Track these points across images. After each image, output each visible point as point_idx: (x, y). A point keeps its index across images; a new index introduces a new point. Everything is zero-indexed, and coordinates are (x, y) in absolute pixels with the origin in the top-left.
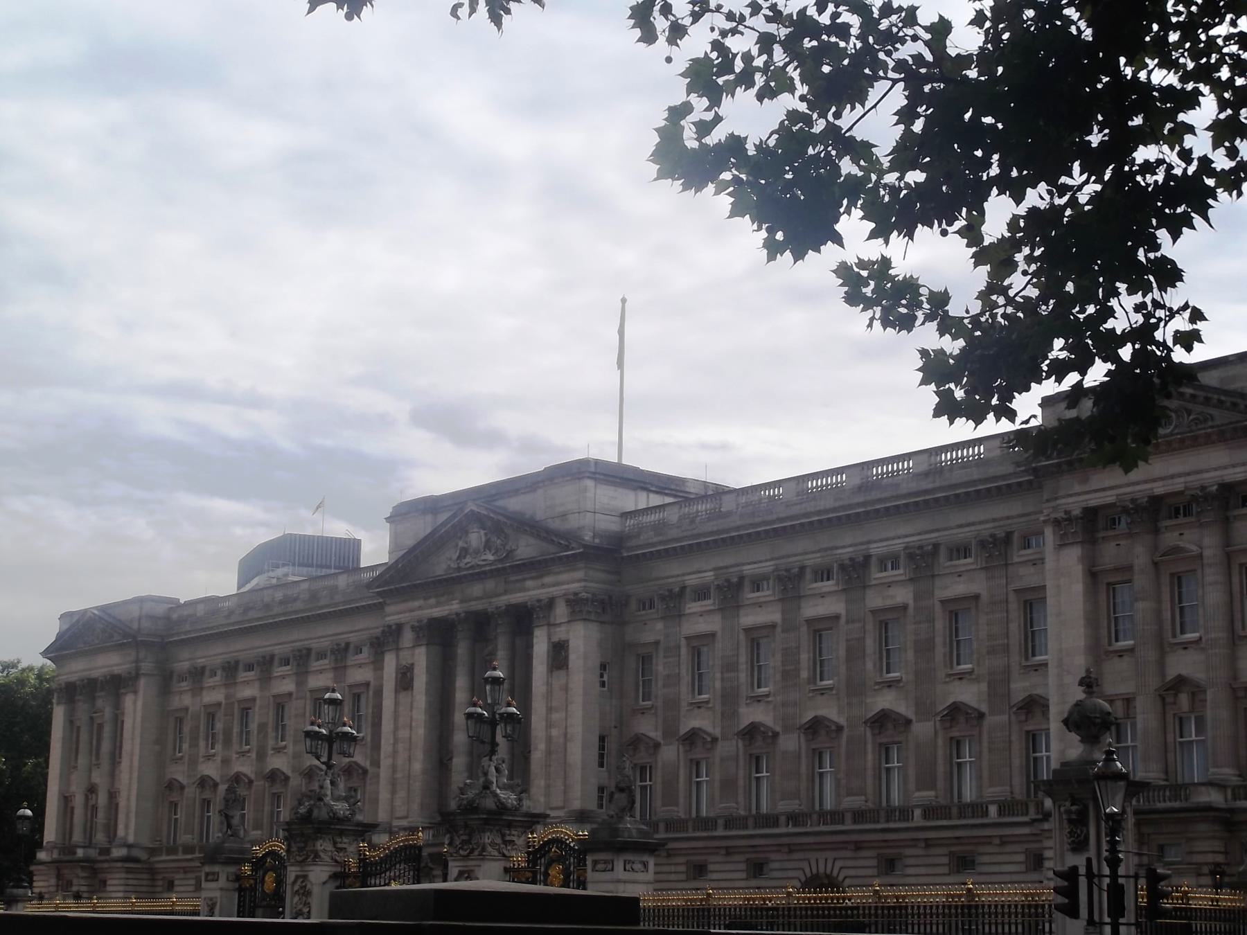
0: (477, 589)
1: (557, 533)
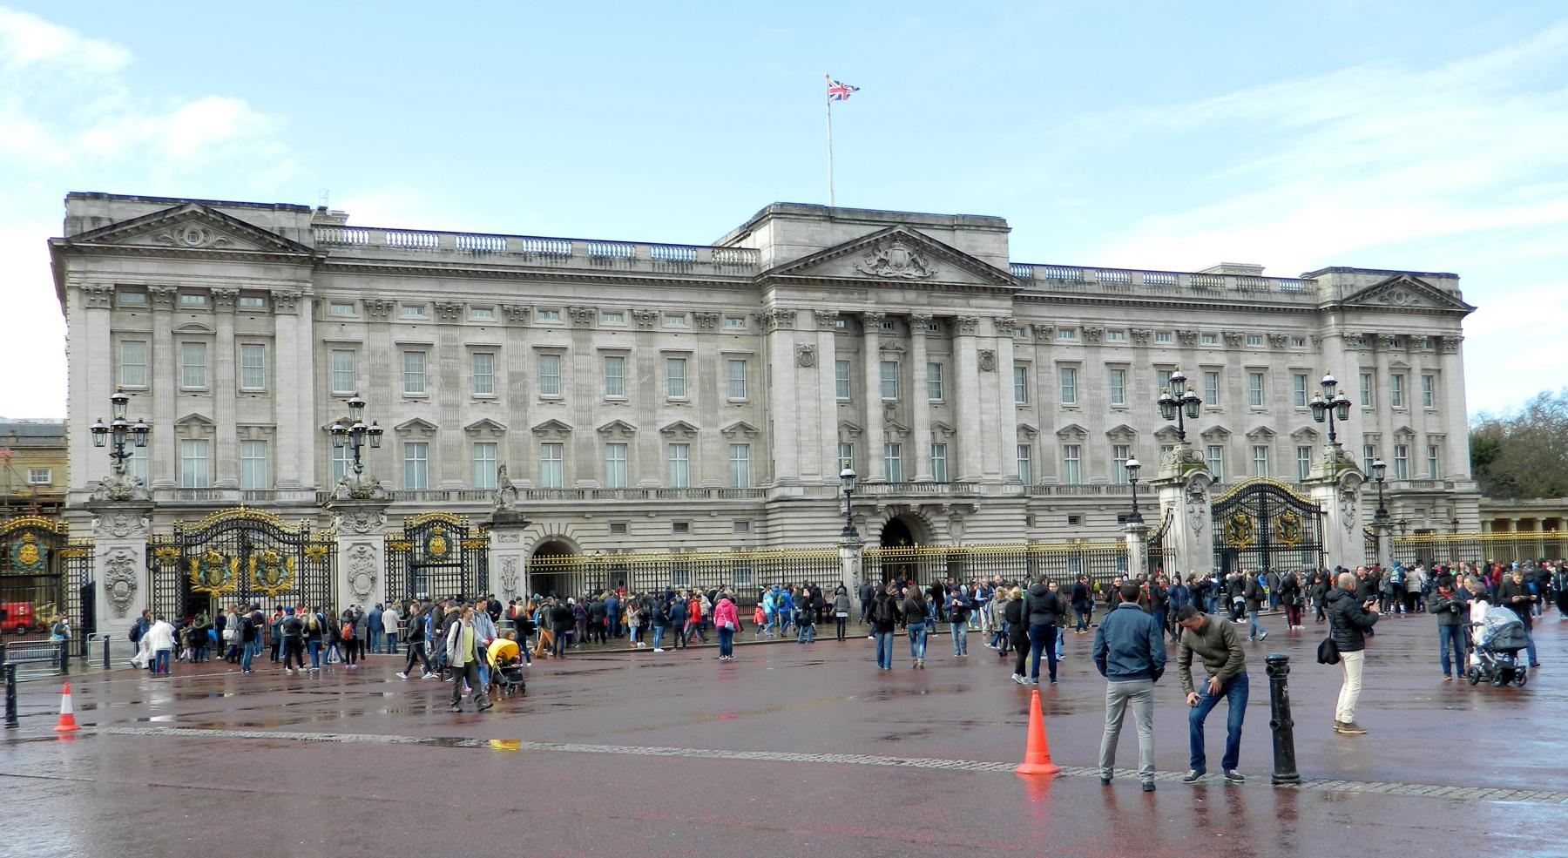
0: (896, 296)
1: (1000, 271)
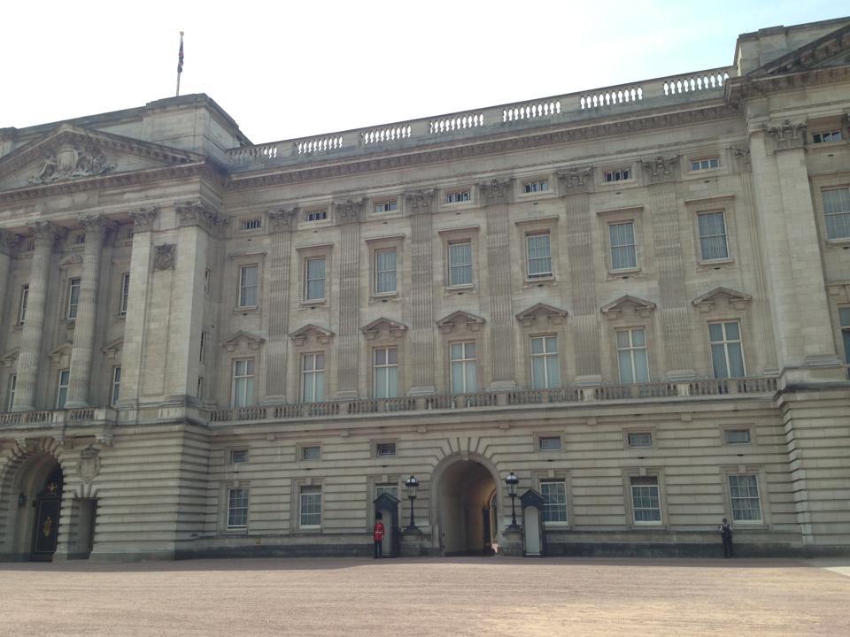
0: (65, 201)
1: (172, 150)
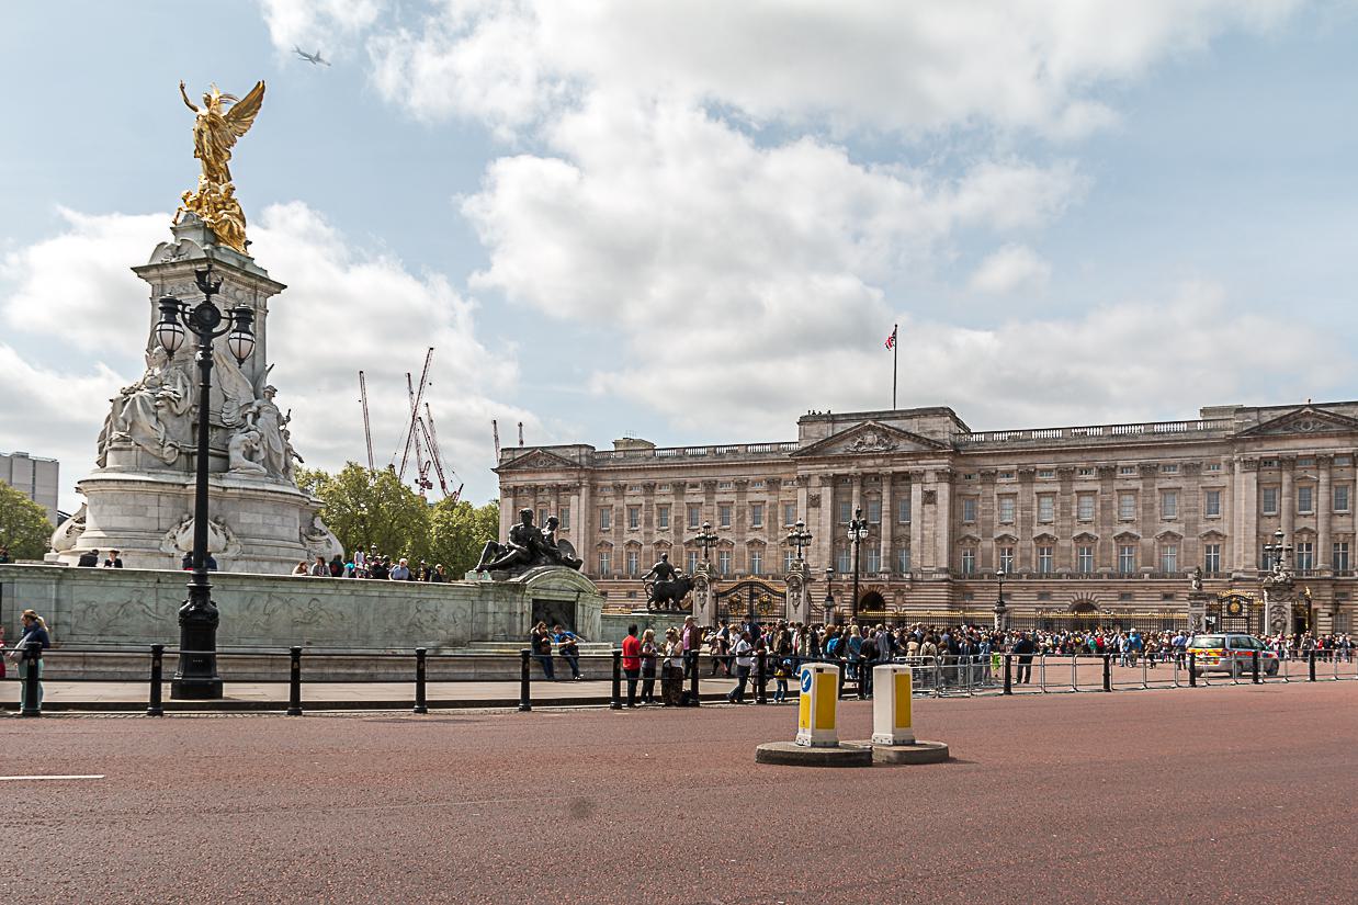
0: (870, 462)
1: (935, 442)
